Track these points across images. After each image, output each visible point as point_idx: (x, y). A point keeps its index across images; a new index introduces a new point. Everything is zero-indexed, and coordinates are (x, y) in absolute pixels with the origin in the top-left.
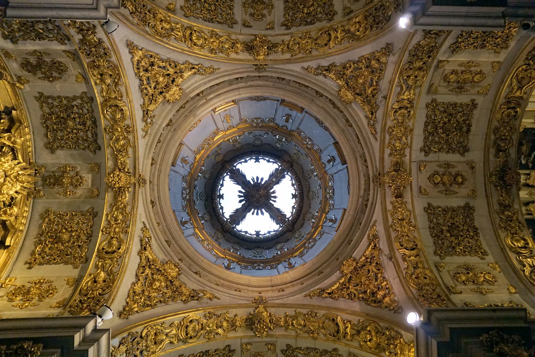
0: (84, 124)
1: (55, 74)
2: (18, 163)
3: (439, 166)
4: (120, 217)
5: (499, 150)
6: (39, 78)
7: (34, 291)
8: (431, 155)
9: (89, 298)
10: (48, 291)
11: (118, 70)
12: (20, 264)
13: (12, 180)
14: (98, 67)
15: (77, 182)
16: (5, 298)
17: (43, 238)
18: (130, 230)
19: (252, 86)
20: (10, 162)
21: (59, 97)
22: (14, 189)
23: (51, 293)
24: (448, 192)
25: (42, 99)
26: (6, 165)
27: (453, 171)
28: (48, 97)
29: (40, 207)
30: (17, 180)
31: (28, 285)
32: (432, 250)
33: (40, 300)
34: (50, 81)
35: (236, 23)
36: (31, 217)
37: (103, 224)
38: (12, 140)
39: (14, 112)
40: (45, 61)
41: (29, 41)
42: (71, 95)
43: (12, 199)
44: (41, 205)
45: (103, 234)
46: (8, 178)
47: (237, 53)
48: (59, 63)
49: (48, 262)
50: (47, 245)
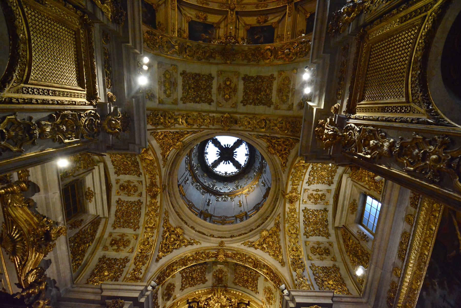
0: (194, 270)
3: (220, 94)
4: (239, 256)
5: (211, 56)
7: (268, 296)
8: (213, 98)
12: (257, 296)
15: (221, 271)
18: (245, 253)
19: (172, 187)
20: (212, 301)
21: (182, 282)
24: (235, 90)
27: (223, 86)
28: (182, 286)
31: (266, 296)
32: (268, 108)
33: (273, 294)
35: (140, 200)
39: (190, 301)
43: (228, 299)
44: (230, 284)
47: (157, 202)
48: (167, 287)
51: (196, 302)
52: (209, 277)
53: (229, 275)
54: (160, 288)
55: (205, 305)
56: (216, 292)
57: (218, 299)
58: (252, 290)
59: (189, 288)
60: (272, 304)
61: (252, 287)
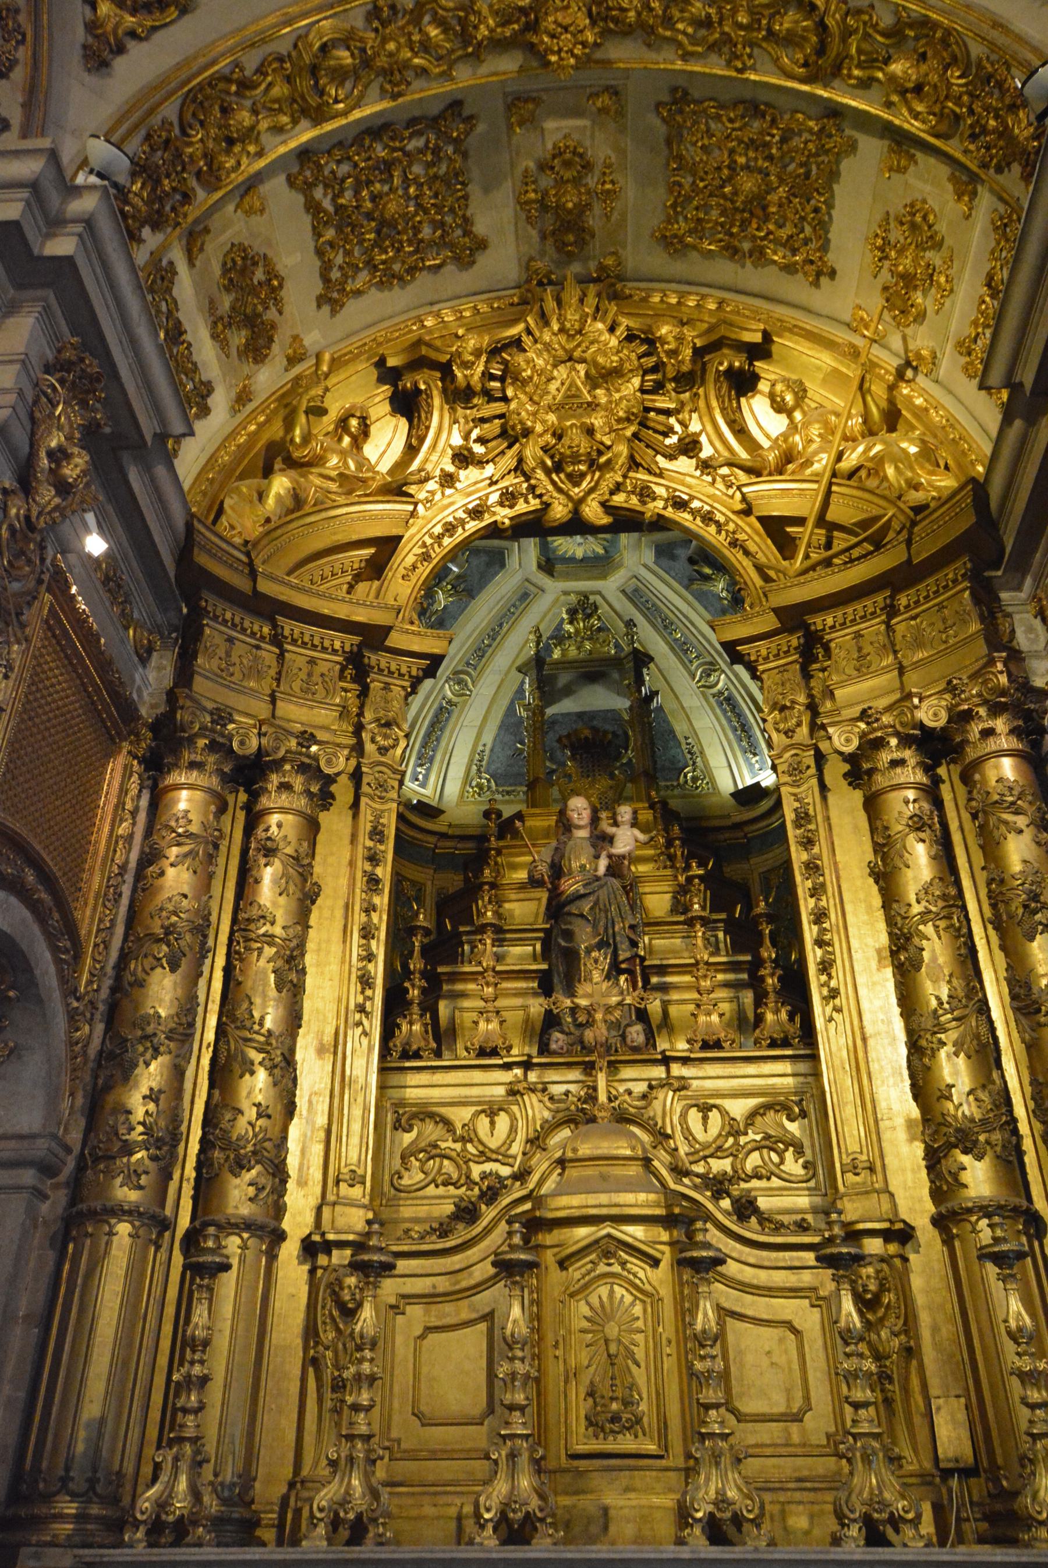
0: (388, 166)
1: (259, 275)
2: (529, 332)
6: (281, 313)
7: (906, 264)
9: (971, 112)
10: (914, 227)
11: (200, 87)
13: (579, 345)
14: (209, 157)
15: (572, 161)
16: (909, 331)
17: (746, 246)
20: (531, 354)
21: (319, 253)
22: (606, 336)
23: (925, 218)
25: (335, 295)
26: (540, 362)
28: (326, 280)
29: (657, 261)
30: (579, 332)
31: (885, 276)
33: (938, 246)
34: (281, 286)
36: (679, 282)
37: (717, 67)
38: (471, 358)
39: (391, 362)
40: (233, 308)
41: (195, 358)
42: (307, 220)
43: (630, 338)
44: (641, 255)
45: (753, 68)
46: (577, 354)
48: (226, 271)
49: (822, 227)
50: (770, 233)
51: (434, 365)
52: (495, 215)
53: (631, 193)
54: (177, 255)
55: (493, 377)
56: (550, 304)
57: (571, 337)
58: (789, 269)
59: (374, 294)
60: (921, 317)
61: (790, 245)
